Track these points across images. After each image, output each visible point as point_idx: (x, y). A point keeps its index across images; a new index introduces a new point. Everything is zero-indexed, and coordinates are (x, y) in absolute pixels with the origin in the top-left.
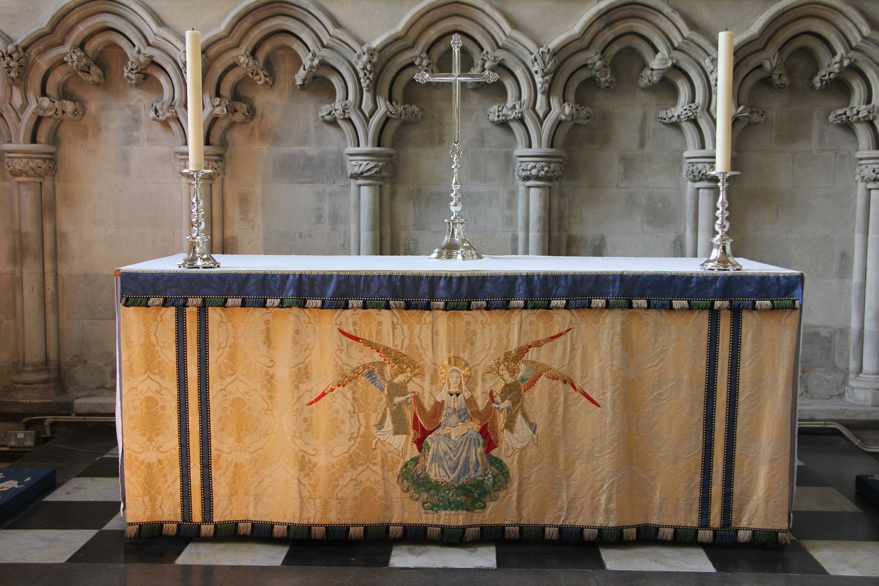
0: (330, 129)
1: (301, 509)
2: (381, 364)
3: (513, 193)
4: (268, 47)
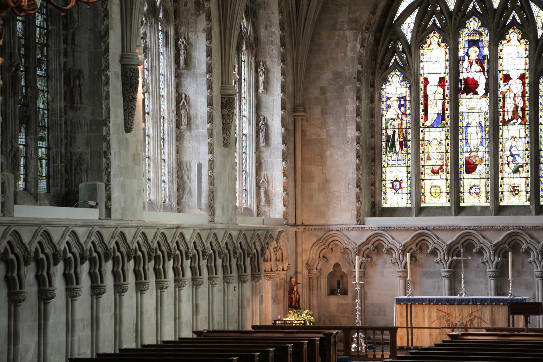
0: (437, 264)
1: (430, 343)
2: (445, 316)
3: (487, 281)
4: (420, 244)
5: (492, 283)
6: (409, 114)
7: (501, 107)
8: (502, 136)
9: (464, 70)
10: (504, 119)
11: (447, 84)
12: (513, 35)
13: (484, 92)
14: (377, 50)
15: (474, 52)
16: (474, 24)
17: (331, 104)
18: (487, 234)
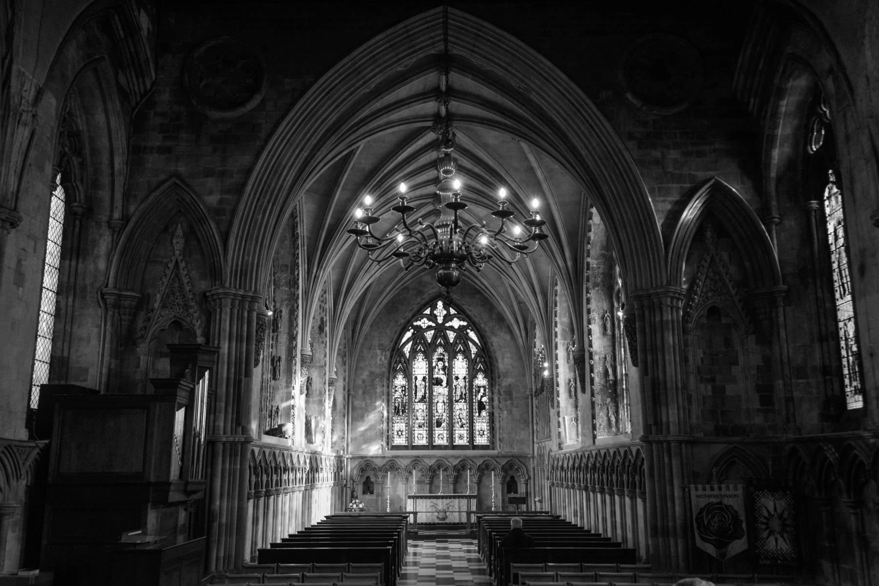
5: (452, 487)
11: (427, 380)
12: (460, 357)
13: (446, 385)
15: (441, 364)
17: (368, 388)
18: (450, 460)
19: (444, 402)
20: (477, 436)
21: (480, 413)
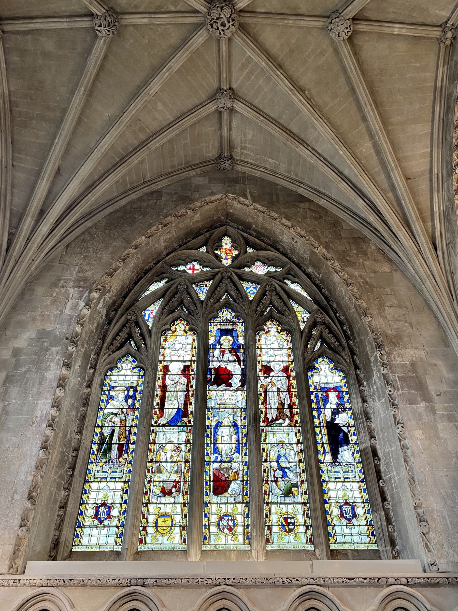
6: (138, 408)
7: (262, 404)
8: (264, 440)
9: (215, 359)
10: (267, 419)
11: (193, 374)
14: (108, 330)
15: (227, 341)
16: (227, 314)
19: (235, 424)
20: (336, 521)
21: (335, 454)
